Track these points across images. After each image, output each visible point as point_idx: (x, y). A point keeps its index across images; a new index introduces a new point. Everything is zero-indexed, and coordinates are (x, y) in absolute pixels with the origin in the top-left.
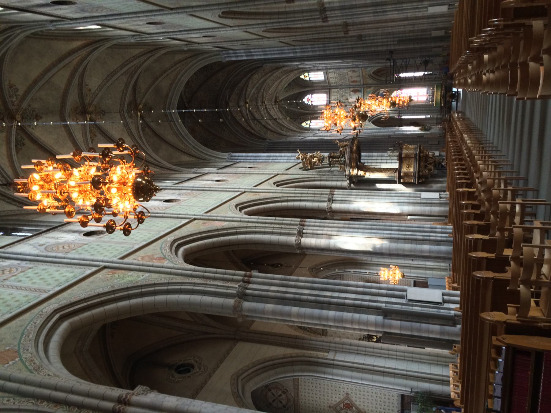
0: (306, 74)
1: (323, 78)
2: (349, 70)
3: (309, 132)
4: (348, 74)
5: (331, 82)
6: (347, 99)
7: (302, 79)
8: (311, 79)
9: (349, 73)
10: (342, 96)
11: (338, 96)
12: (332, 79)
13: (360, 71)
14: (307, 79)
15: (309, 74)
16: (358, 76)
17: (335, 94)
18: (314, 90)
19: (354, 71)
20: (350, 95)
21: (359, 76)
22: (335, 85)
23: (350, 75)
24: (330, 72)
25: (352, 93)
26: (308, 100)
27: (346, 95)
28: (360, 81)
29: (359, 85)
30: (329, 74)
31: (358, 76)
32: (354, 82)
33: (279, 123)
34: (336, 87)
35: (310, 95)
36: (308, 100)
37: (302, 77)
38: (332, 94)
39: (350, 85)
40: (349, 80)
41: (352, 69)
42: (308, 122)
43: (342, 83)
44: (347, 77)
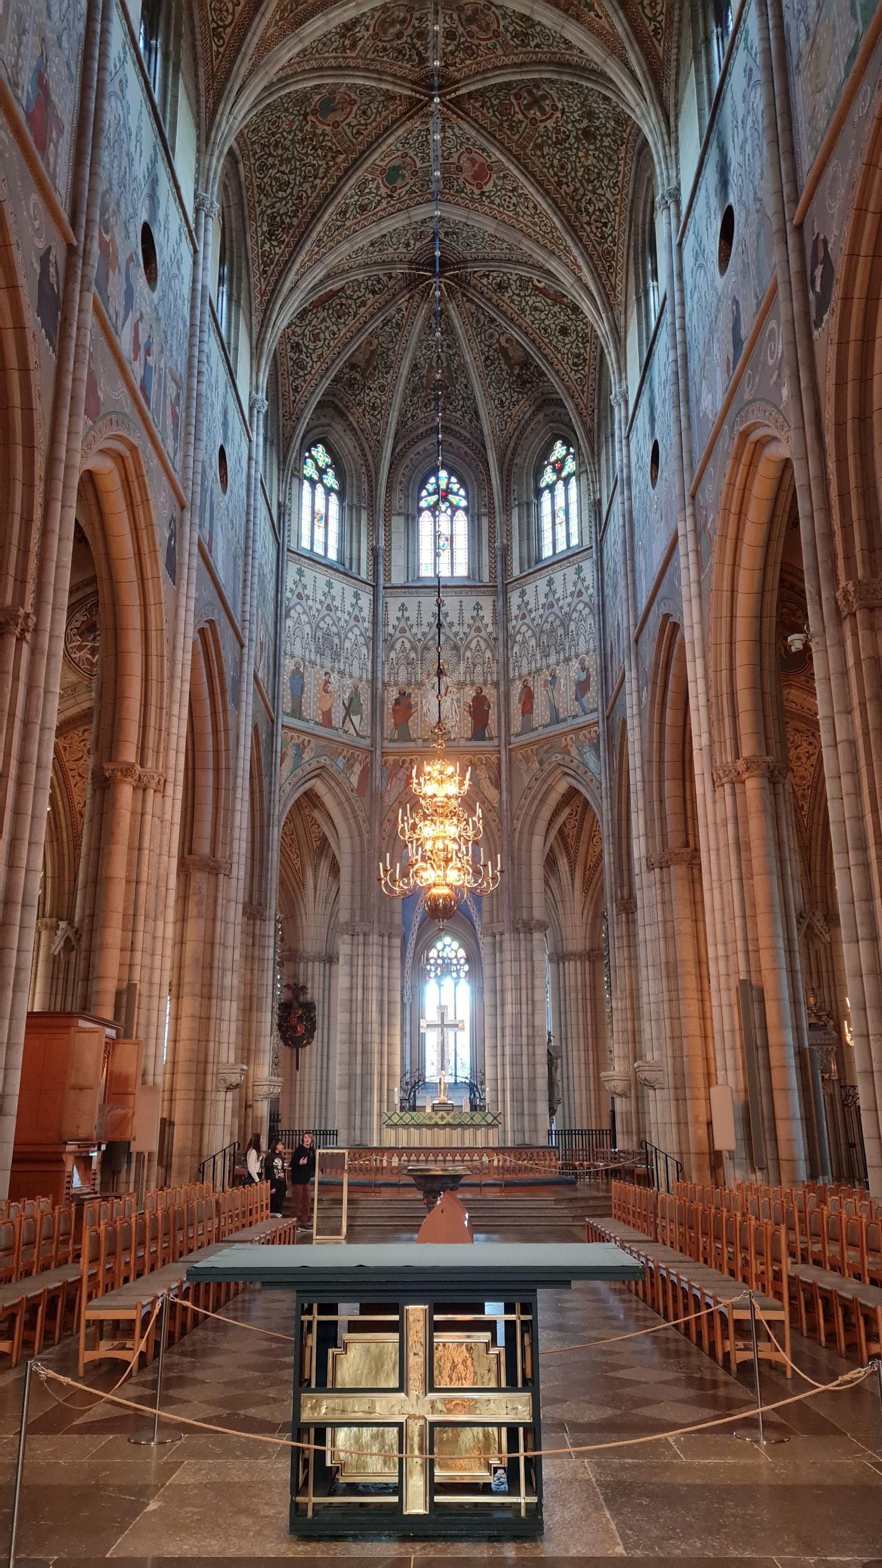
0: (570, 466)
1: (547, 552)
2: (593, 662)
3: (262, 395)
4: (567, 660)
5: (530, 589)
7: (549, 449)
8: (546, 496)
9: (575, 664)
10: (456, 648)
11: (454, 629)
12: (543, 588)
14: (549, 476)
15: (573, 479)
16: (555, 711)
17: (468, 614)
18: (491, 514)
19: (582, 687)
20: (461, 685)
21: (556, 719)
22: (514, 611)
24: (579, 570)
25: (471, 692)
26: (444, 495)
27: (462, 667)
28: (527, 728)
29: (508, 729)
30: (570, 572)
31: (555, 711)
32: (528, 697)
33: (315, 215)
34: (502, 616)
35: (463, 503)
36: (444, 495)
37: (559, 450)
38: (469, 602)
39: (509, 682)
40: (539, 671)
41: (594, 680)
42: (330, 479)
43: (525, 642)
44: (552, 660)
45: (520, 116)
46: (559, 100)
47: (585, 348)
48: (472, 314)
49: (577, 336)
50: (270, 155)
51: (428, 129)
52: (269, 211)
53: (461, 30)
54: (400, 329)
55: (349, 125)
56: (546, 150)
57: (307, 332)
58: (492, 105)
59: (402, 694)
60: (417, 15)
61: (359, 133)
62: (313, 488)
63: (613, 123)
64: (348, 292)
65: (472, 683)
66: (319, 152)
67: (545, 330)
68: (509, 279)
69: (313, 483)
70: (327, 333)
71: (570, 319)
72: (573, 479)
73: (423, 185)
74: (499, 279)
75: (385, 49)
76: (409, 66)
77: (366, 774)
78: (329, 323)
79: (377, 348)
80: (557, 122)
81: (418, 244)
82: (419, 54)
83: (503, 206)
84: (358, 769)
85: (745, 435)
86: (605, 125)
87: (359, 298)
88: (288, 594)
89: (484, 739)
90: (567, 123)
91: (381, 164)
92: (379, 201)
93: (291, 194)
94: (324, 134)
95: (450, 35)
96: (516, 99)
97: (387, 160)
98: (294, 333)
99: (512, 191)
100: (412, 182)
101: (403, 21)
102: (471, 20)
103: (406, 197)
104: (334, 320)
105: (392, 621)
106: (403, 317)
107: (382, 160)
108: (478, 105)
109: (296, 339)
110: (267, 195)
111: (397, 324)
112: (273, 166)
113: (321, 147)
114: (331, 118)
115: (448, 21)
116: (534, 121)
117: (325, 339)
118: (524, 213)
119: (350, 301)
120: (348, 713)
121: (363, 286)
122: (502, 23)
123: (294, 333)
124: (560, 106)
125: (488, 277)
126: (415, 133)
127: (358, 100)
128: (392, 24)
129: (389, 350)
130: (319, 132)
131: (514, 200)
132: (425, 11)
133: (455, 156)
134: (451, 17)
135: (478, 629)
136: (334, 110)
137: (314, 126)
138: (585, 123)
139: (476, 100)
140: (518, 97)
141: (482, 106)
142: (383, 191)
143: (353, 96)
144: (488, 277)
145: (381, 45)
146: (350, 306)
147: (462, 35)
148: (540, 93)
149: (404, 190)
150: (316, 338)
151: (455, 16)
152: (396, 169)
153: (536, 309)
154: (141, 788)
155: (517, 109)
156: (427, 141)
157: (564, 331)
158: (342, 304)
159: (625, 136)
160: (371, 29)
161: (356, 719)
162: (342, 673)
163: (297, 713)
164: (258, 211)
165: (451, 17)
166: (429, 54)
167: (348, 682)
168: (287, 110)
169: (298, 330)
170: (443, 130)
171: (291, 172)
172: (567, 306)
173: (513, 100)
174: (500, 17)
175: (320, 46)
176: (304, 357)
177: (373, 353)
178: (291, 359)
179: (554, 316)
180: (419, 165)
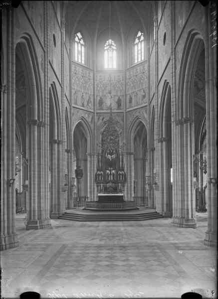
0: (142, 38)
1: (136, 61)
6: (110, 93)
8: (136, 46)
11: (114, 81)
13: (144, 105)
14: (137, 41)
15: (143, 42)
19: (144, 97)
21: (137, 104)
23: (138, 92)
25: (117, 98)
26: (110, 45)
30: (141, 67)
32: (131, 98)
35: (115, 48)
37: (139, 34)
39: (126, 95)
40: (133, 92)
42: (82, 42)
44: (137, 90)
59: (101, 98)
62: (78, 45)
65: (117, 96)
69: (78, 43)
72: (143, 42)
77: (93, 118)
84: (91, 117)
85: (190, 32)
88: (72, 73)
89: (120, 109)
105: (98, 79)
120: (88, 102)
135: (119, 82)
154: (39, 127)
161: (90, 105)
162: (86, 93)
163: (76, 103)
167: (88, 95)
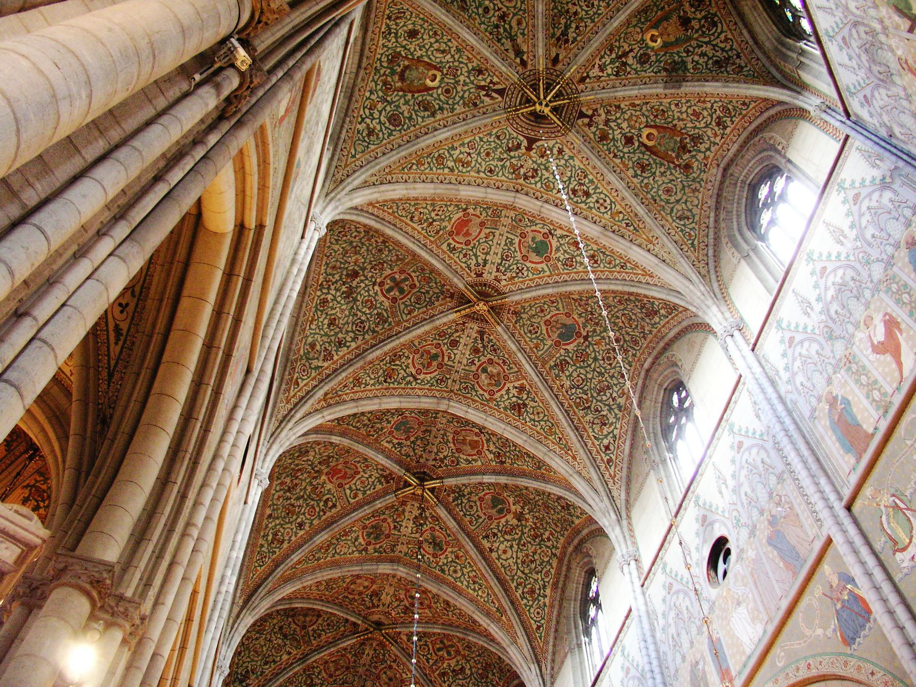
45: (413, 274)
46: (376, 294)
47: (388, 25)
48: (523, 34)
49: (396, 34)
50: (625, 341)
51: (498, 270)
52: (648, 320)
53: (444, 349)
54: (612, 45)
55: (558, 309)
56: (394, 258)
57: (702, 125)
58: (436, 283)
60: (474, 368)
61: (553, 302)
63: (330, 297)
64: (644, 120)
66: (589, 309)
67: (435, 33)
68: (468, 77)
70: (684, 109)
71: (404, 47)
73: (520, 220)
74: (480, 77)
75: (504, 362)
76: (492, 337)
78: (676, 115)
79: (647, 30)
80: (381, 275)
81: (551, 143)
82: (482, 339)
83: (446, 205)
86: (337, 290)
87: (636, 111)
90: (372, 277)
91: (546, 269)
92: (562, 237)
93: (625, 309)
94: (580, 315)
95: (454, 344)
96: (415, 285)
97: (539, 266)
98: (716, 135)
99: (434, 221)
100: (528, 229)
101: (485, 370)
102: (435, 357)
103: (538, 222)
104: (670, 113)
106: (602, 57)
107: (543, 270)
108: (448, 287)
109: (716, 128)
110: (643, 327)
111: (611, 51)
112: (628, 334)
113: (586, 310)
114: (569, 321)
115: (453, 356)
116: (402, 272)
117: (690, 107)
118: (426, 208)
119: (646, 113)
121: (626, 117)
122: (410, 361)
123: (716, 135)
124: (377, 288)
125: (491, 82)
126: (509, 275)
127: (542, 324)
128: (491, 376)
129: (634, 26)
130: (583, 319)
131: (433, 214)
132: (467, 368)
133: (482, 235)
134: (449, 357)
136: (564, 325)
137: (585, 326)
138: (354, 284)
139: (448, 290)
140: (413, 286)
141: (444, 285)
142: (555, 243)
143: (544, 328)
144: (491, 82)
145: (505, 367)
146: (647, 110)
147: (444, 344)
148: (392, 293)
149: (537, 228)
150: (696, 114)
151: (446, 359)
152: (538, 252)
153: (443, 52)
155: (415, 279)
156: (502, 259)
157: (413, 34)
158: (656, 116)
159: (319, 293)
160: (506, 388)
164: (655, 330)
165: (449, 357)
166: (476, 335)
168: (595, 359)
169: (709, 133)
170: (485, 262)
171: (618, 317)
172: (406, 58)
173: (418, 284)
174: (411, 365)
175: (542, 415)
176: (718, 112)
177: (655, 26)
178: (733, 122)
179: (424, 46)
180: (517, 240)
